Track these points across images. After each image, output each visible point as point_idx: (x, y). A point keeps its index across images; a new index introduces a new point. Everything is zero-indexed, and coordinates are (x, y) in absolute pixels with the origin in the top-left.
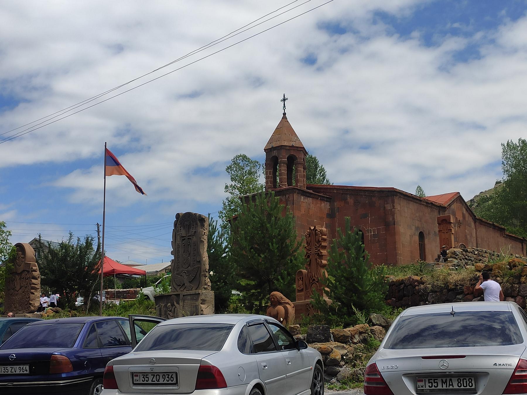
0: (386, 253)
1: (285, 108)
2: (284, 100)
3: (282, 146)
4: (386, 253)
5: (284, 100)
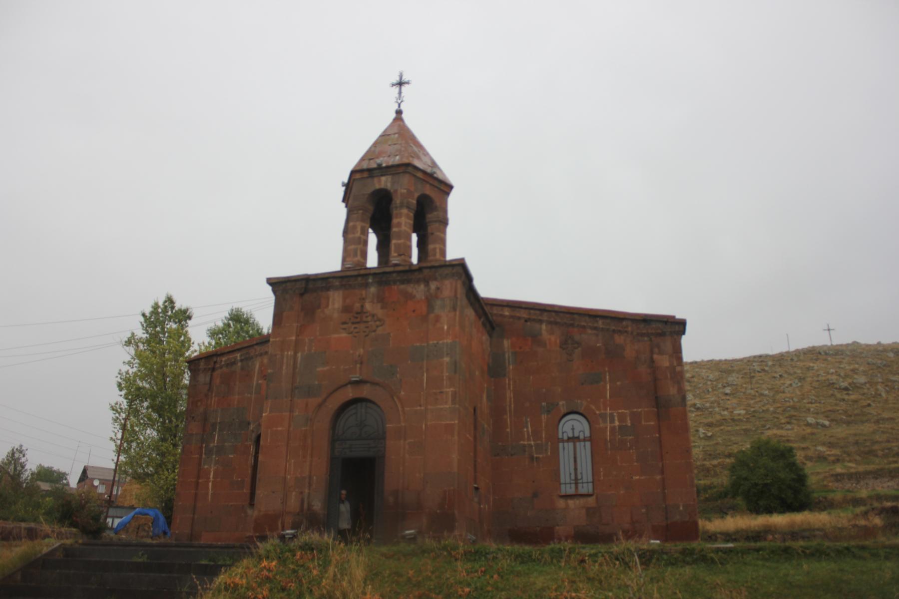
0: (659, 477)
1: (402, 101)
2: (400, 84)
3: (408, 165)
4: (659, 477)
5: (400, 84)
